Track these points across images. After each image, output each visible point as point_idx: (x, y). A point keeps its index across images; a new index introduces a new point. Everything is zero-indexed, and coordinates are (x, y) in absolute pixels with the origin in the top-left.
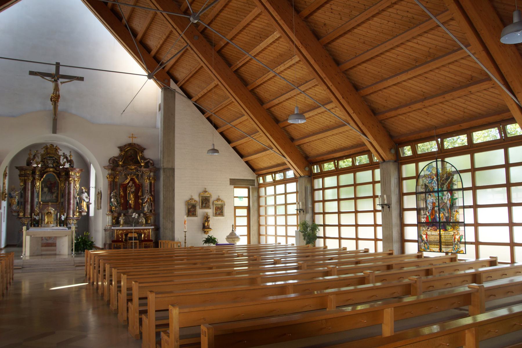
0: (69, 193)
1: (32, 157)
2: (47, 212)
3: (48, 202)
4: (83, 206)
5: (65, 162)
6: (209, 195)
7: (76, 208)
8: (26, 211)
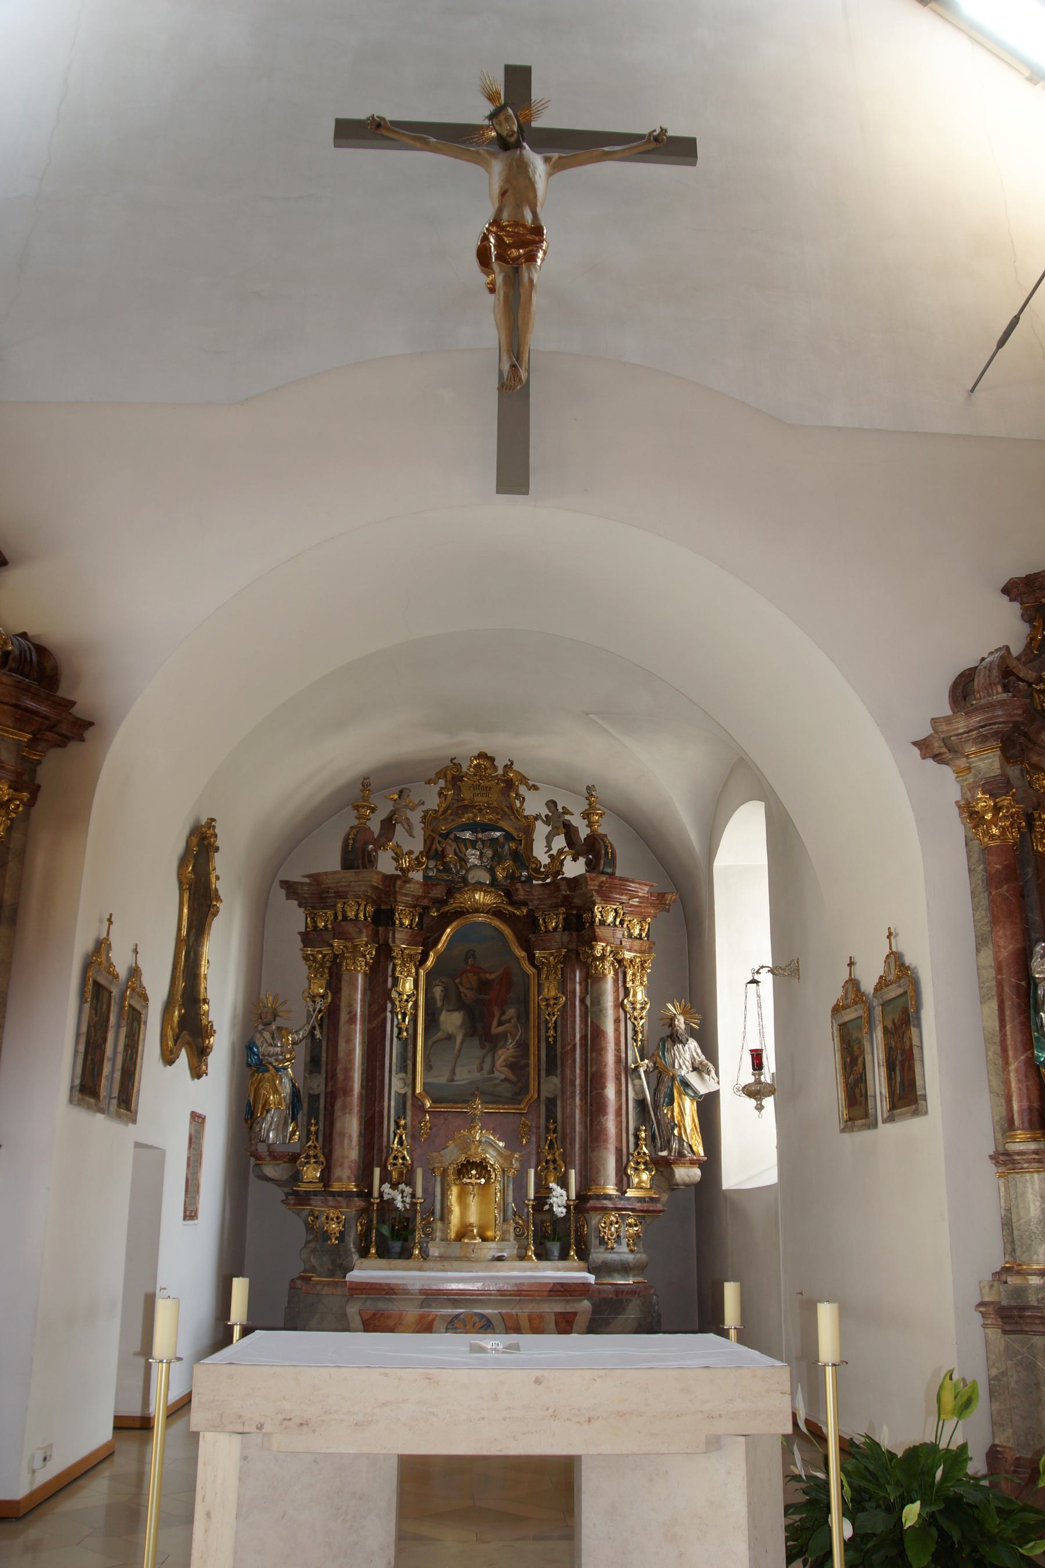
0: (594, 1037)
1: (375, 826)
2: (462, 1159)
3: (464, 1098)
4: (681, 1126)
5: (561, 852)
7: (637, 1137)
8: (337, 1153)
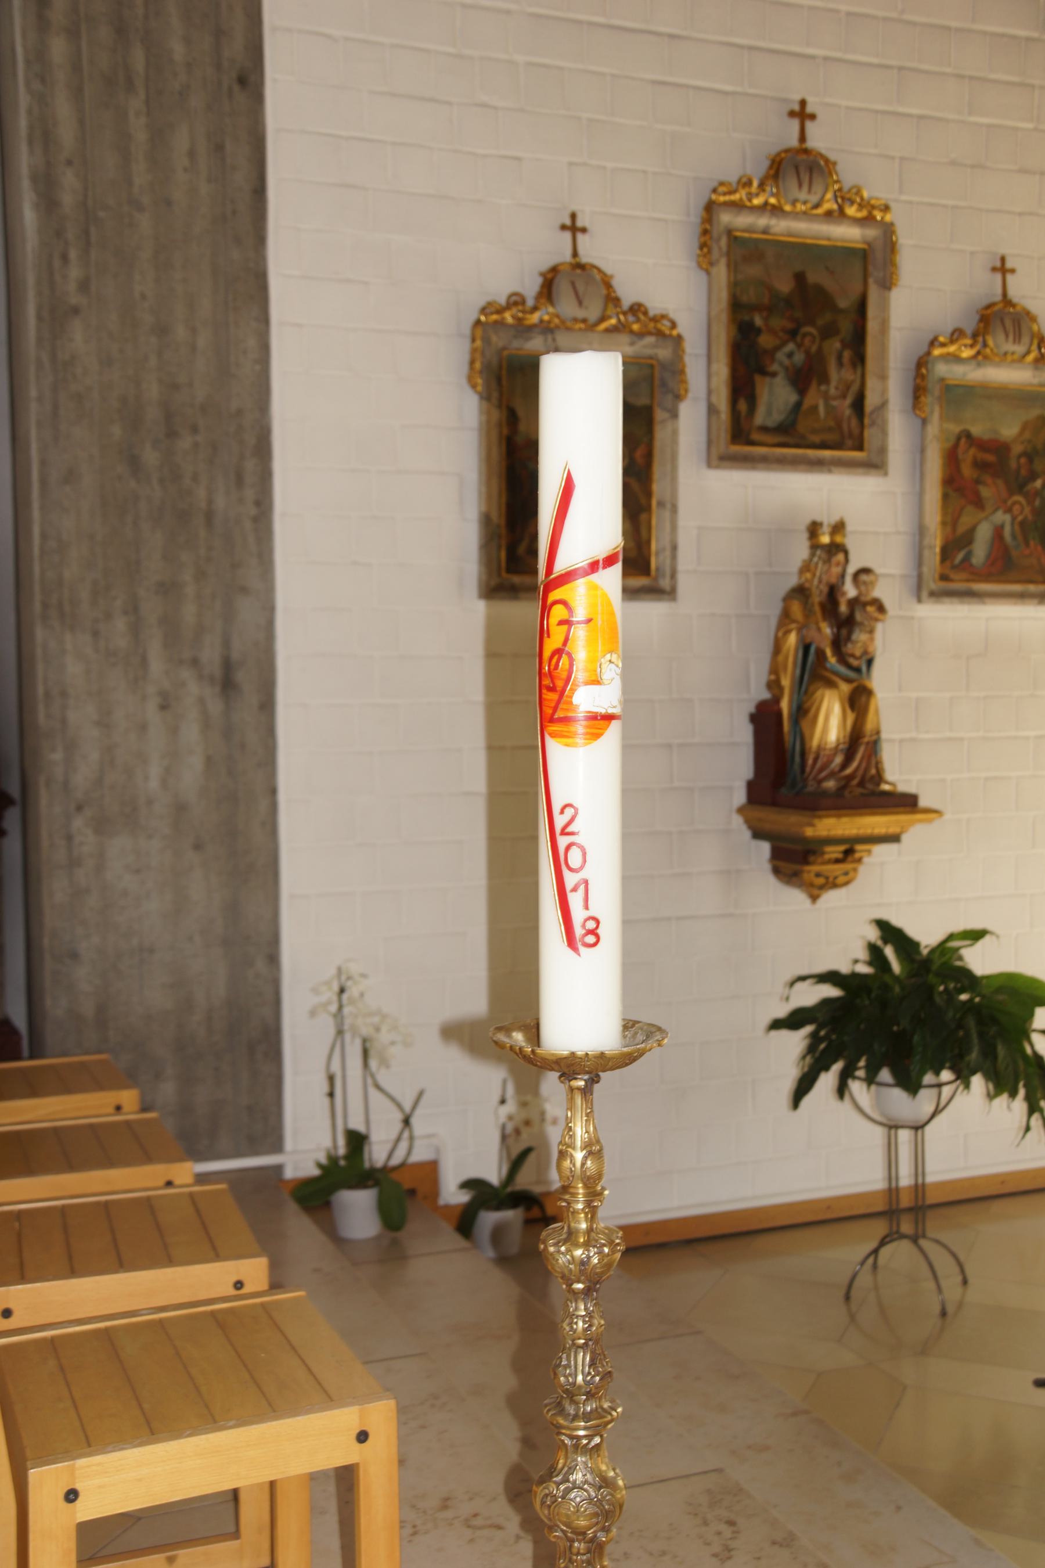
6: (847, 233)
